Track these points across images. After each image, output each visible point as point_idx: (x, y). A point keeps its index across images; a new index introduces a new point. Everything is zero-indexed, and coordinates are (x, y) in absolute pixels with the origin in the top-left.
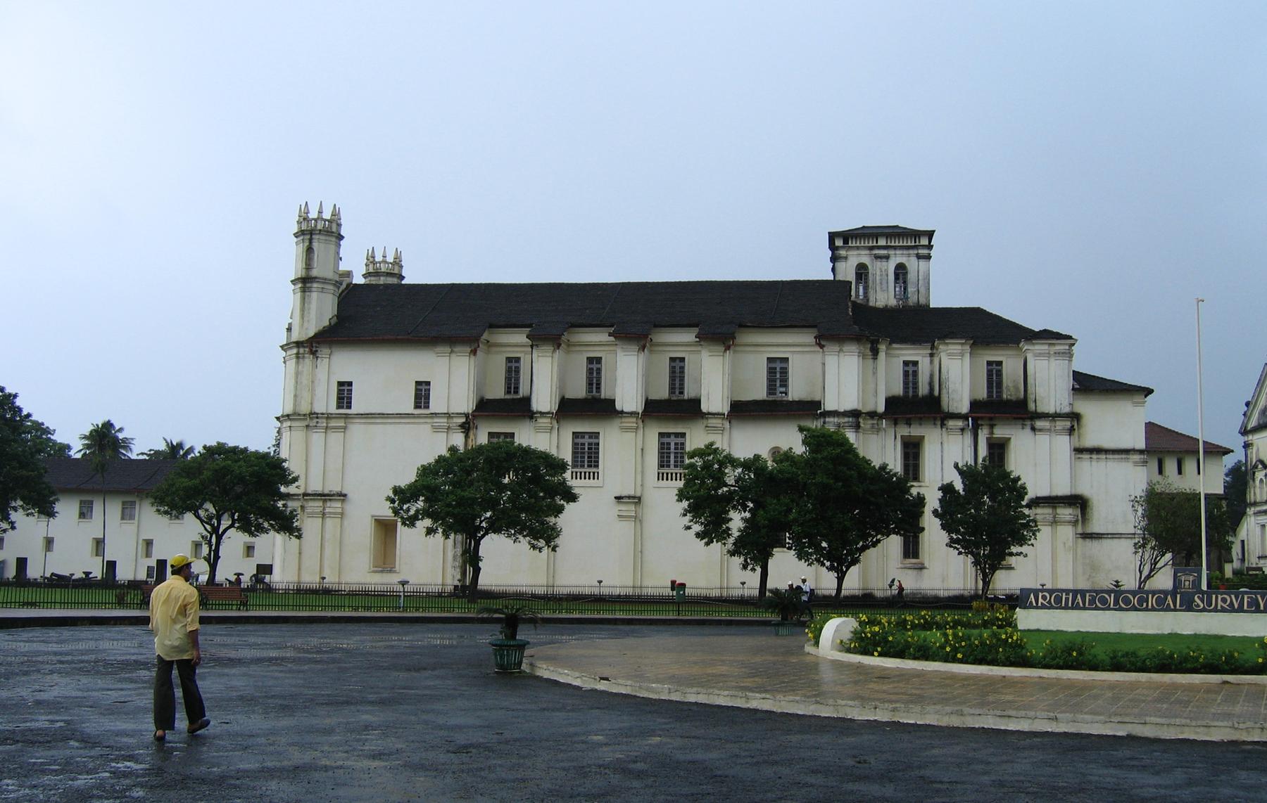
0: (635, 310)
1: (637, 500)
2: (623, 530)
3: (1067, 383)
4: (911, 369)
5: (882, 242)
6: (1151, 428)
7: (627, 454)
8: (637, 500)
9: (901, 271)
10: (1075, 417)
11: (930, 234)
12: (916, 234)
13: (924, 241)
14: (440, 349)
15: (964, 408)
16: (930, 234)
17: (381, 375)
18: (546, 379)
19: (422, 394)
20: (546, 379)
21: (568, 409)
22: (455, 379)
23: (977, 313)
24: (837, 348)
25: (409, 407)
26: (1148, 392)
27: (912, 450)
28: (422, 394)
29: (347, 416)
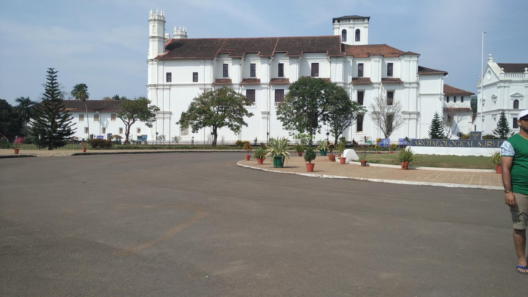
0: (267, 48)
1: (268, 113)
2: (264, 123)
3: (415, 70)
4: (360, 67)
5: (351, 22)
6: (445, 86)
7: (265, 98)
8: (268, 113)
9: (358, 32)
10: (418, 84)
11: (368, 18)
12: (363, 19)
13: (366, 21)
15: (380, 80)
16: (368, 18)
17: (182, 72)
18: (235, 72)
20: (235, 72)
21: (245, 81)
22: (207, 72)
23: (385, 45)
24: (335, 59)
25: (191, 81)
27: (361, 95)
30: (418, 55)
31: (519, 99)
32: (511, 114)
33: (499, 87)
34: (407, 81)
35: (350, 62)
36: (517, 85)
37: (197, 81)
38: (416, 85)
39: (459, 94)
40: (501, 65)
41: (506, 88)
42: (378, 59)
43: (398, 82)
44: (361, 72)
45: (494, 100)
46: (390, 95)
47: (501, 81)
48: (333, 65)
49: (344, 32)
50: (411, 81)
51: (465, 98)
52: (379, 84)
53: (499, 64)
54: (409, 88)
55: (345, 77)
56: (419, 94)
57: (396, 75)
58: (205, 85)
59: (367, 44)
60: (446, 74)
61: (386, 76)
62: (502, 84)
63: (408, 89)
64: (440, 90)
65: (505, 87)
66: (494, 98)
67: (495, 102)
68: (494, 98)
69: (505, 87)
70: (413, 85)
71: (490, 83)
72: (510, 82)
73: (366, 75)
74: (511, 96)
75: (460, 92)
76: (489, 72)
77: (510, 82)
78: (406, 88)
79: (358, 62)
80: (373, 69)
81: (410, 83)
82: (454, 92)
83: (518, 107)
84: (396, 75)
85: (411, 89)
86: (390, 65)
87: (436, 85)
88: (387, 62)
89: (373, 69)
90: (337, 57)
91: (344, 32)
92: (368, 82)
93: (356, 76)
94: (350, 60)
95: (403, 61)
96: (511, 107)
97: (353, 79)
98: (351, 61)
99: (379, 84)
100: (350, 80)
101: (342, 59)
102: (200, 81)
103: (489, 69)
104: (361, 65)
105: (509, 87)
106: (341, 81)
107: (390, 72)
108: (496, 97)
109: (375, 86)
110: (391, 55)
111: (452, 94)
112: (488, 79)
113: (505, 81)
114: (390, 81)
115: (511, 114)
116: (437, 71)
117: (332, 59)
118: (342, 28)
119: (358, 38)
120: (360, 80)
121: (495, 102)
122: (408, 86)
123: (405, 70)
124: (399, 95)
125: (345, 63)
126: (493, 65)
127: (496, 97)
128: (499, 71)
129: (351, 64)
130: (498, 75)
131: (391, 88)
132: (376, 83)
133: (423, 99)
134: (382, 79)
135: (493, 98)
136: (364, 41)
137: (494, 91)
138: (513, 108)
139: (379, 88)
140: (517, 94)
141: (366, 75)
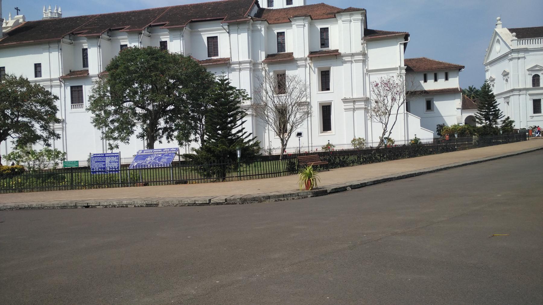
10: (364, 54)
15: (307, 54)
24: (236, 27)
31: (539, 73)
32: (530, 95)
33: (511, 60)
34: (348, 52)
35: (261, 30)
36: (536, 55)
38: (361, 57)
41: (520, 60)
43: (336, 55)
44: (281, 45)
45: (506, 78)
47: (513, 51)
48: (234, 36)
50: (354, 51)
54: (351, 62)
56: (368, 71)
61: (318, 47)
63: (349, 65)
65: (519, 58)
67: (507, 80)
68: (506, 74)
69: (519, 58)
70: (357, 58)
71: (499, 55)
73: (288, 49)
74: (528, 70)
75: (442, 65)
77: (526, 50)
78: (345, 62)
79: (277, 31)
81: (352, 55)
82: (434, 66)
83: (538, 84)
85: (354, 64)
87: (390, 57)
88: (320, 26)
89: (297, 39)
90: (239, 24)
92: (290, 59)
93: (275, 51)
96: (530, 85)
97: (268, 56)
98: (263, 29)
99: (305, 60)
100: (262, 56)
101: (246, 27)
105: (524, 58)
106: (247, 59)
107: (324, 42)
108: (508, 74)
109: (299, 63)
110: (325, 16)
111: (431, 70)
112: (498, 50)
114: (324, 55)
115: (530, 95)
117: (231, 28)
121: (507, 80)
122: (349, 59)
124: (337, 73)
125: (253, 32)
127: (508, 74)
129: (263, 33)
131: (324, 65)
132: (301, 59)
134: (311, 53)
135: (505, 75)
137: (505, 65)
138: (532, 87)
139: (306, 66)
140: (536, 66)
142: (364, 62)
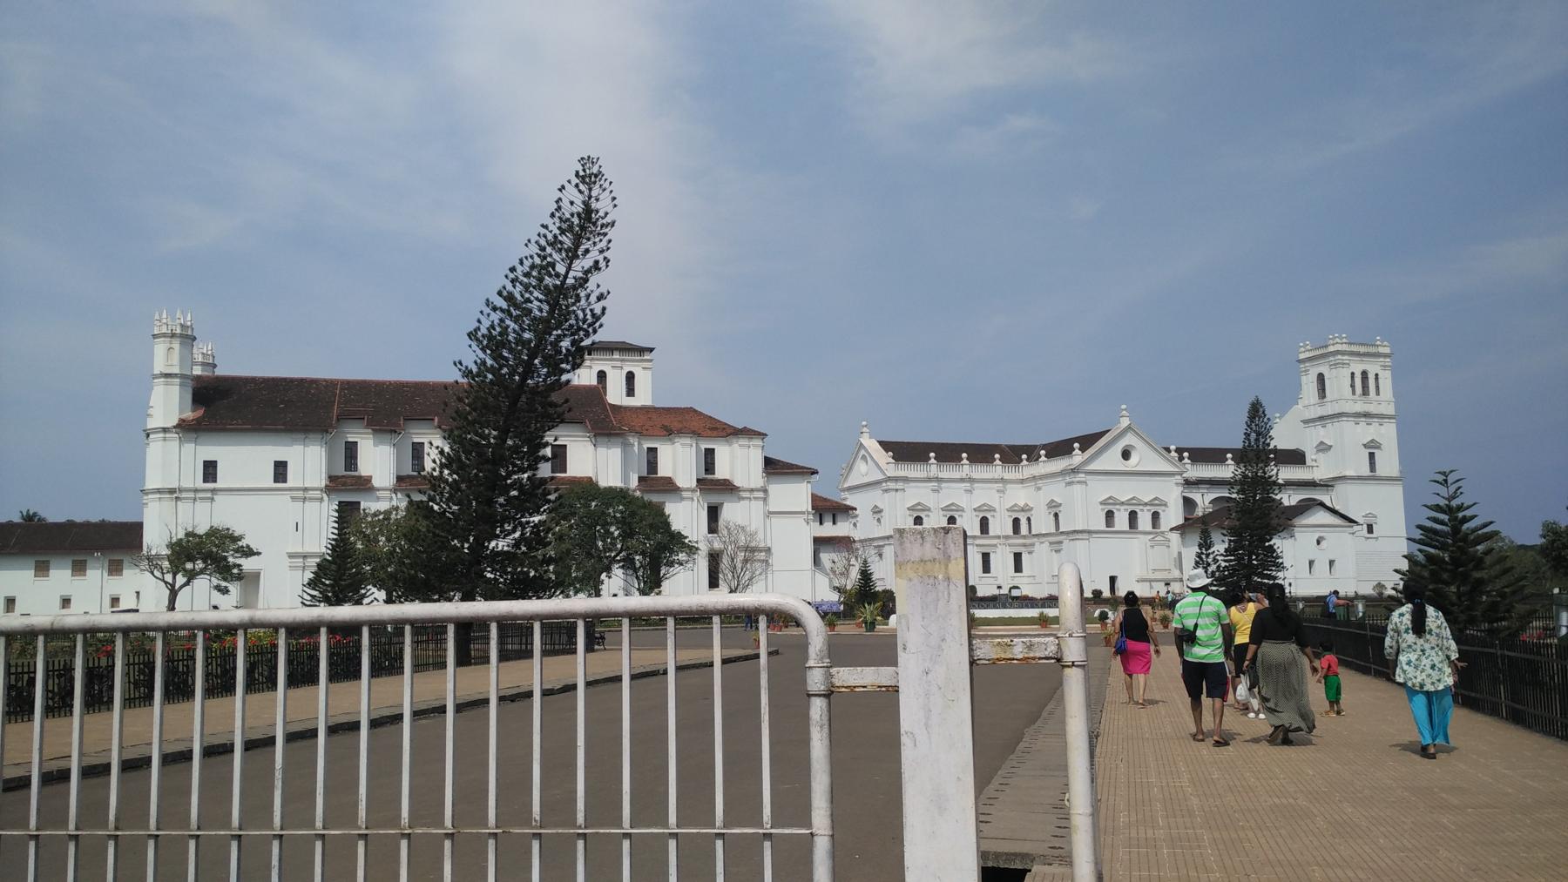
3: (760, 464)
5: (616, 356)
6: (815, 498)
9: (630, 377)
10: (765, 491)
11: (651, 350)
12: (641, 350)
14: (294, 436)
15: (694, 484)
19: (280, 471)
22: (309, 461)
23: (691, 411)
26: (814, 472)
28: (280, 471)
29: (214, 491)
30: (763, 435)
33: (886, 491)
37: (285, 481)
38: (761, 495)
39: (828, 510)
40: (886, 445)
42: (688, 441)
43: (727, 487)
44: (652, 465)
46: (714, 513)
47: (890, 479)
48: (602, 451)
49: (602, 375)
51: (839, 518)
52: (693, 491)
53: (881, 443)
55: (626, 478)
57: (721, 472)
58: (306, 489)
59: (649, 403)
60: (814, 472)
62: (891, 485)
64: (806, 505)
66: (877, 511)
70: (757, 494)
72: (905, 480)
73: (663, 471)
76: (864, 457)
79: (646, 445)
80: (678, 460)
81: (752, 490)
84: (721, 472)
86: (710, 453)
87: (796, 495)
88: (704, 445)
89: (678, 460)
90: (609, 435)
91: (602, 375)
94: (634, 440)
95: (736, 446)
97: (641, 479)
99: (693, 491)
102: (293, 479)
103: (863, 452)
104: (652, 452)
107: (709, 466)
109: (685, 494)
113: (896, 479)
114: (714, 487)
116: (798, 467)
118: (598, 366)
119: (630, 392)
120: (653, 481)
123: (738, 462)
124: (732, 512)
125: (626, 446)
126: (871, 444)
128: (884, 458)
130: (882, 464)
131: (714, 499)
132: (688, 490)
133: (776, 521)
136: (643, 398)
141: (663, 471)
142: (765, 500)
